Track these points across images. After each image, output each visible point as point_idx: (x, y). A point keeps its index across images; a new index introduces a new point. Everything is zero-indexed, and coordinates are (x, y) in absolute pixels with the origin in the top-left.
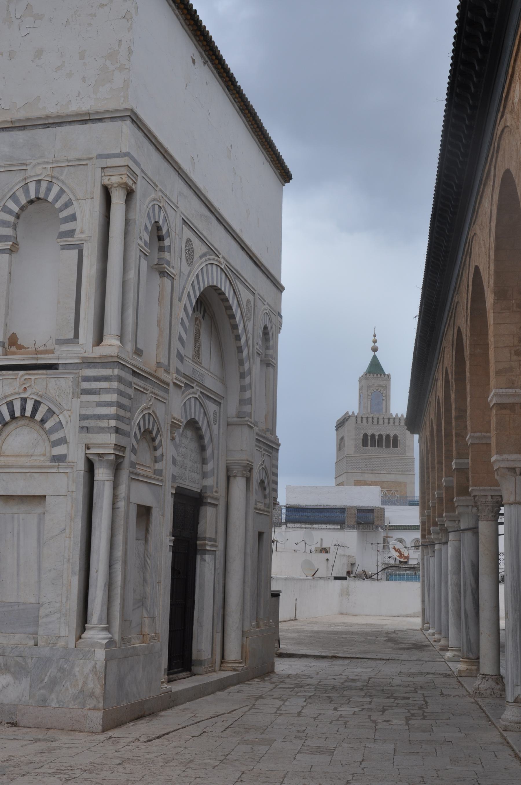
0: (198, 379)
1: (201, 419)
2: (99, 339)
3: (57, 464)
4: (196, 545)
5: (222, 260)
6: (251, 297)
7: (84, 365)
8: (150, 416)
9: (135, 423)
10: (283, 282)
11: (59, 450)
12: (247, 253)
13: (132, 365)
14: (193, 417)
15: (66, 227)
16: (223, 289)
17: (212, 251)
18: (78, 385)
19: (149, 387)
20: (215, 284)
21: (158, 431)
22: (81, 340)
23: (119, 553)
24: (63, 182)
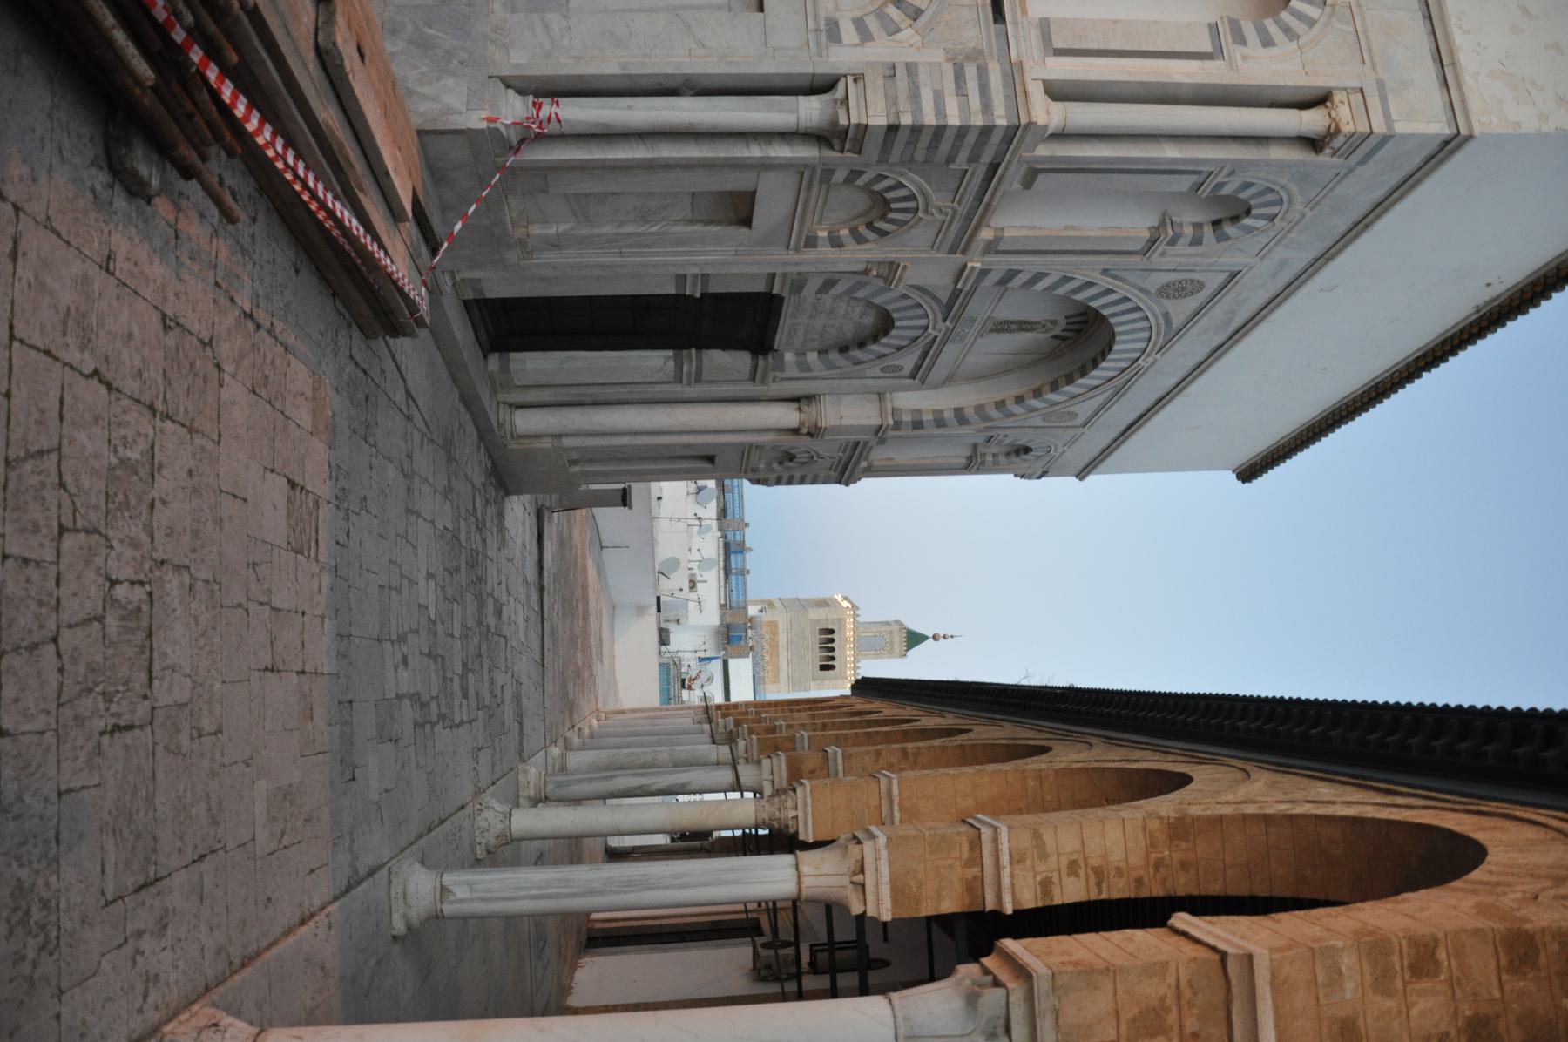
0: (958, 330)
1: (893, 341)
2: (1058, 92)
3: (822, 27)
4: (689, 348)
5: (1150, 360)
6: (1079, 421)
7: (1007, 67)
8: (914, 206)
9: (902, 175)
10: (1091, 478)
11: (849, 33)
12: (1149, 410)
13: (1009, 162)
14: (897, 324)
15: (1249, 29)
16: (1104, 364)
17: (1173, 335)
18: (969, 58)
19: (962, 210)
20: (1116, 347)
21: (883, 234)
22: (1054, 62)
23: (666, 151)
24: (1326, 24)
